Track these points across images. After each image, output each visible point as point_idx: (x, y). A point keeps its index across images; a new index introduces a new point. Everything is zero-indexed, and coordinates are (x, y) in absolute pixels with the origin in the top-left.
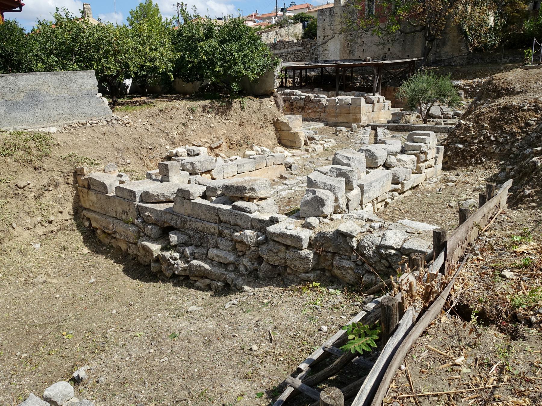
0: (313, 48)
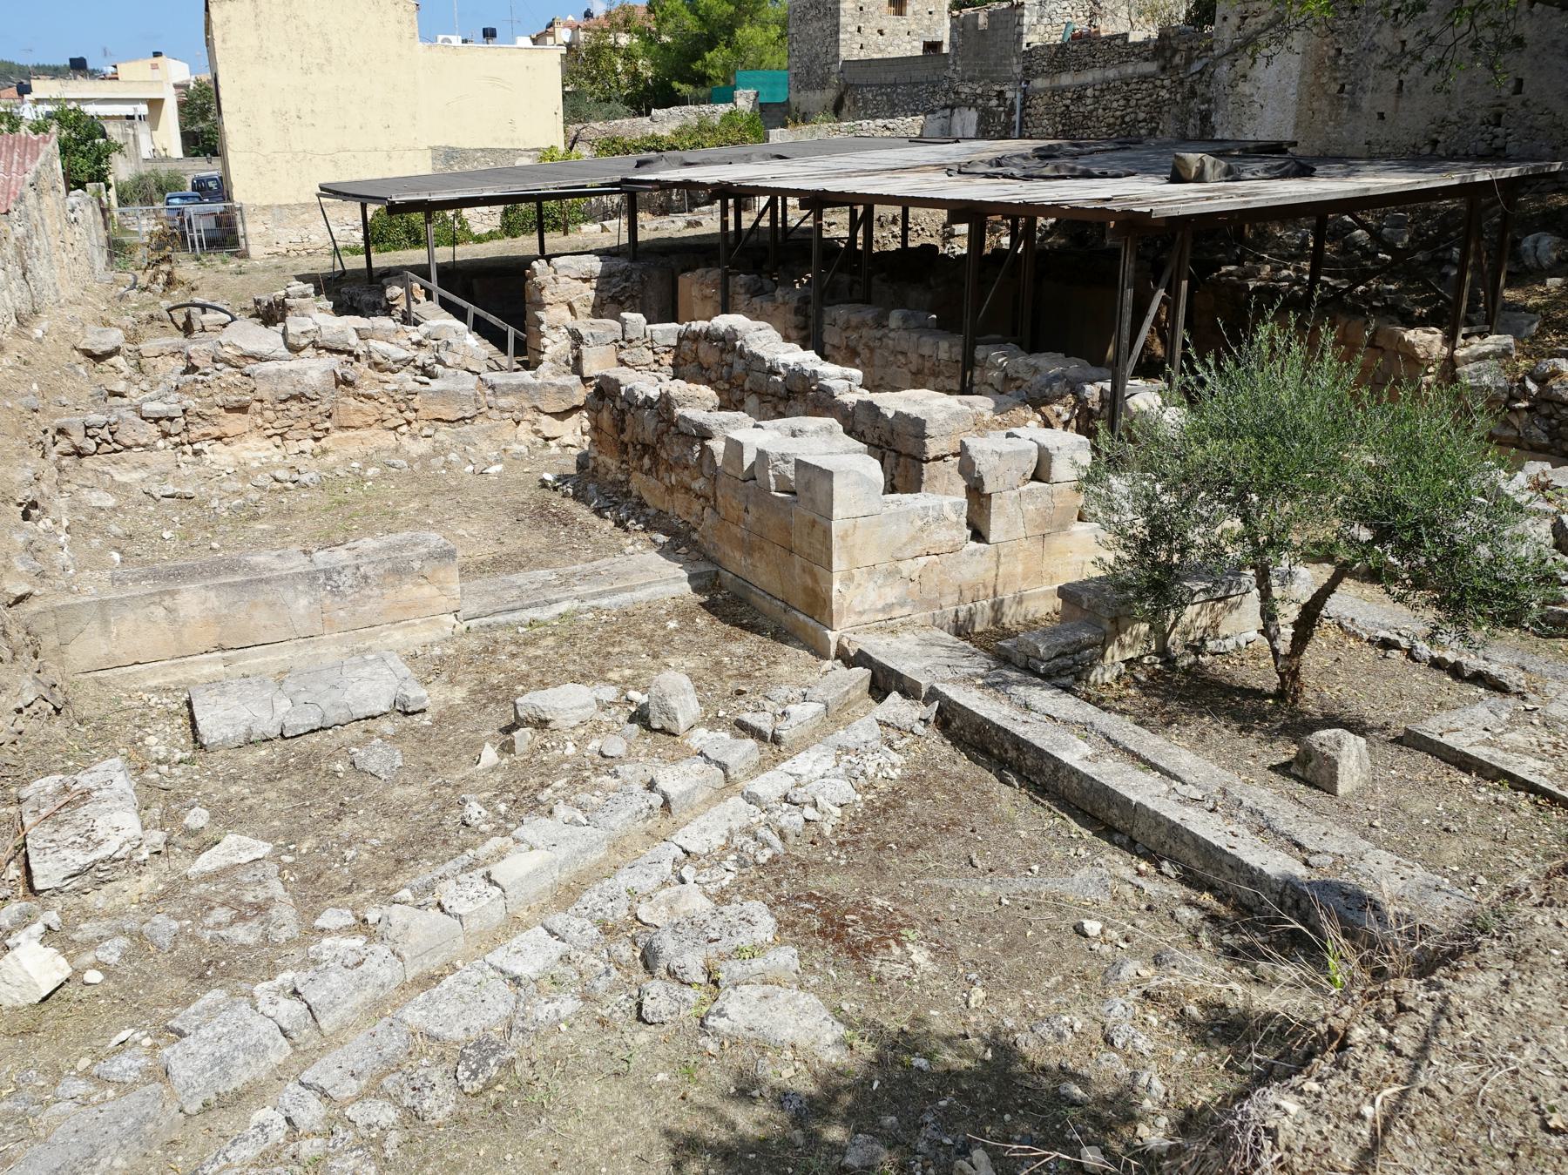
0: (1196, 66)
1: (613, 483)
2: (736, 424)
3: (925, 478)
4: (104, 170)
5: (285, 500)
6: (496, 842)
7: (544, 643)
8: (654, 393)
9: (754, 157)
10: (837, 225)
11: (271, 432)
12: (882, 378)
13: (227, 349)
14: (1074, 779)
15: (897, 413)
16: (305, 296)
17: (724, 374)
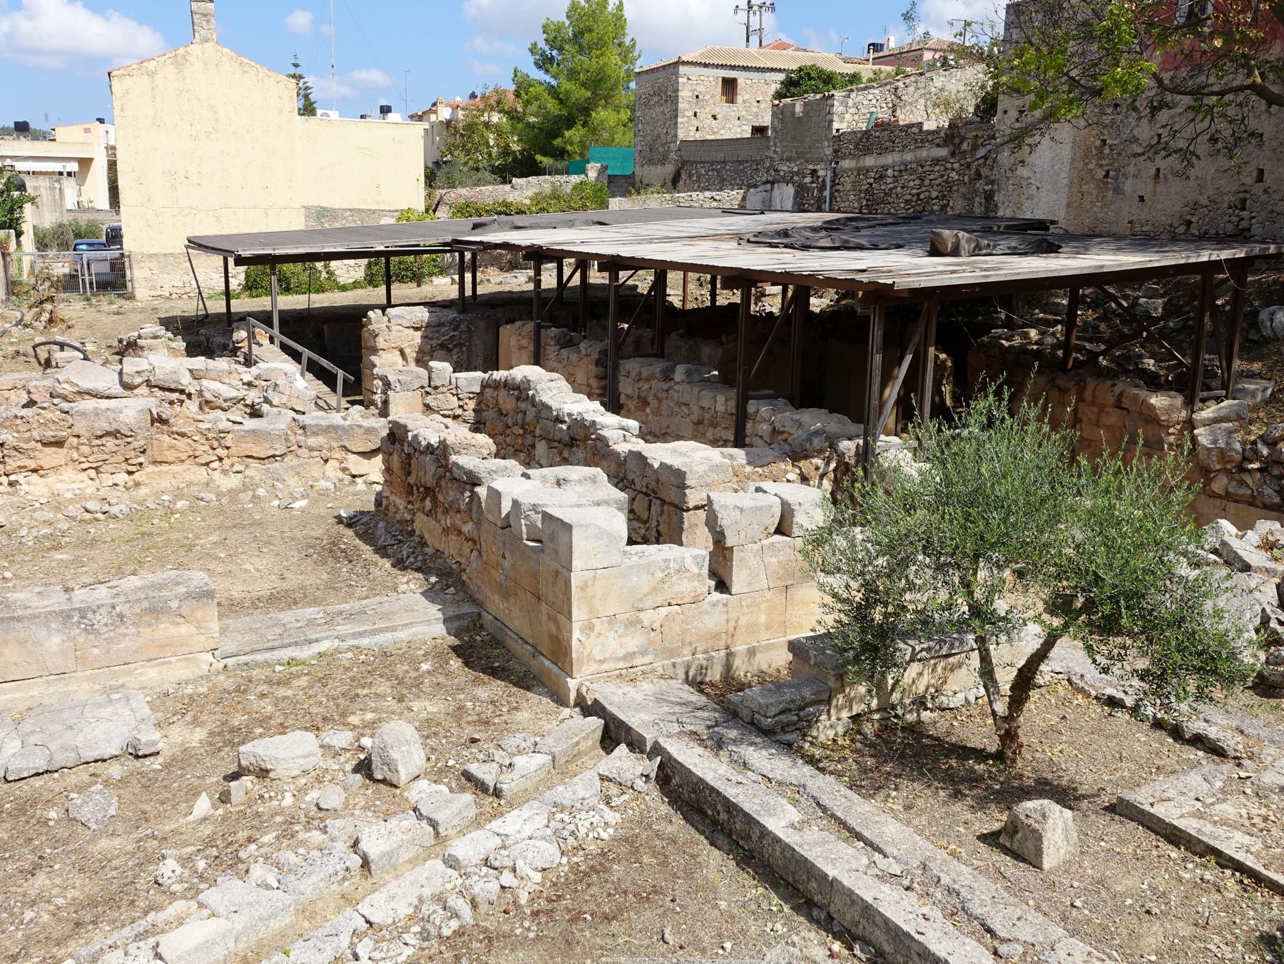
0: (981, 152)
1: (400, 522)
2: (505, 472)
3: (686, 525)
4: (17, 219)
5: (92, 531)
6: (180, 906)
7: (296, 683)
8: (434, 441)
9: (577, 223)
10: (643, 282)
11: (87, 465)
12: (668, 427)
13: (65, 386)
14: (778, 849)
15: (662, 464)
16: (156, 337)
17: (519, 421)
